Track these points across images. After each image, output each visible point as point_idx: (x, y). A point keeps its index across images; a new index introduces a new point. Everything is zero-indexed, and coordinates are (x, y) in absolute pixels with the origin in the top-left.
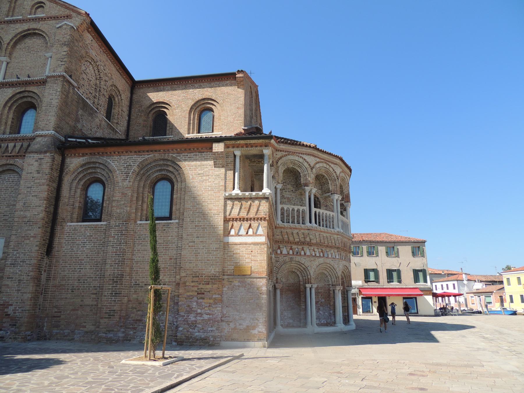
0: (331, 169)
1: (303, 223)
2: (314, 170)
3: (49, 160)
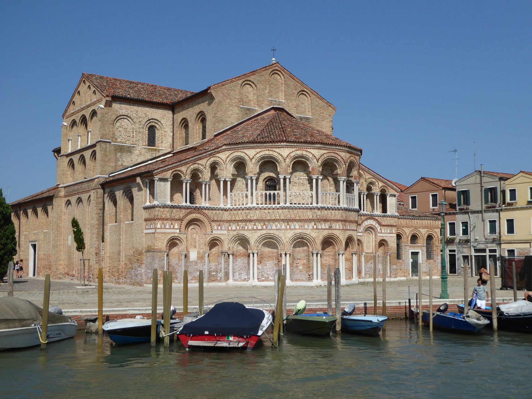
0: (275, 154)
2: (254, 160)
3: (95, 193)
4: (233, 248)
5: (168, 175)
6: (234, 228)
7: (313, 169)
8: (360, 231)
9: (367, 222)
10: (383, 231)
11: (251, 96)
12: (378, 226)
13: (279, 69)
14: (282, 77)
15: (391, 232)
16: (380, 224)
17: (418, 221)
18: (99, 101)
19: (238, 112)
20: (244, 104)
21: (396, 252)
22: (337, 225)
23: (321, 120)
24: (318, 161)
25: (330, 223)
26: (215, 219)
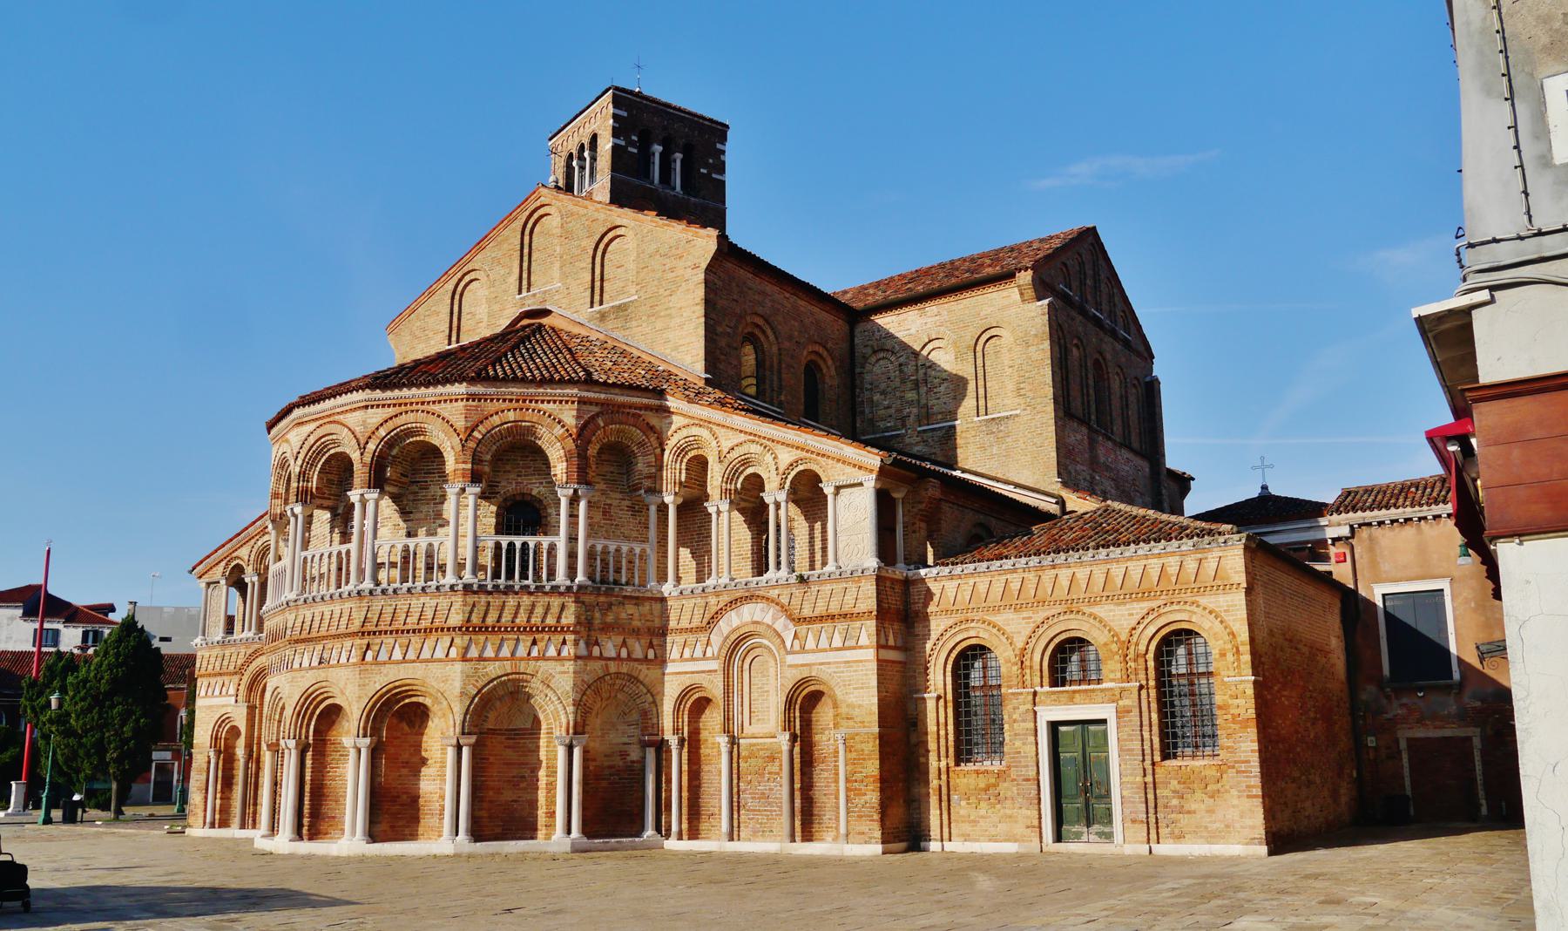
8: (709, 654)
10: (810, 644)
12: (786, 627)
15: (853, 643)
21: (876, 730)
23: (668, 292)
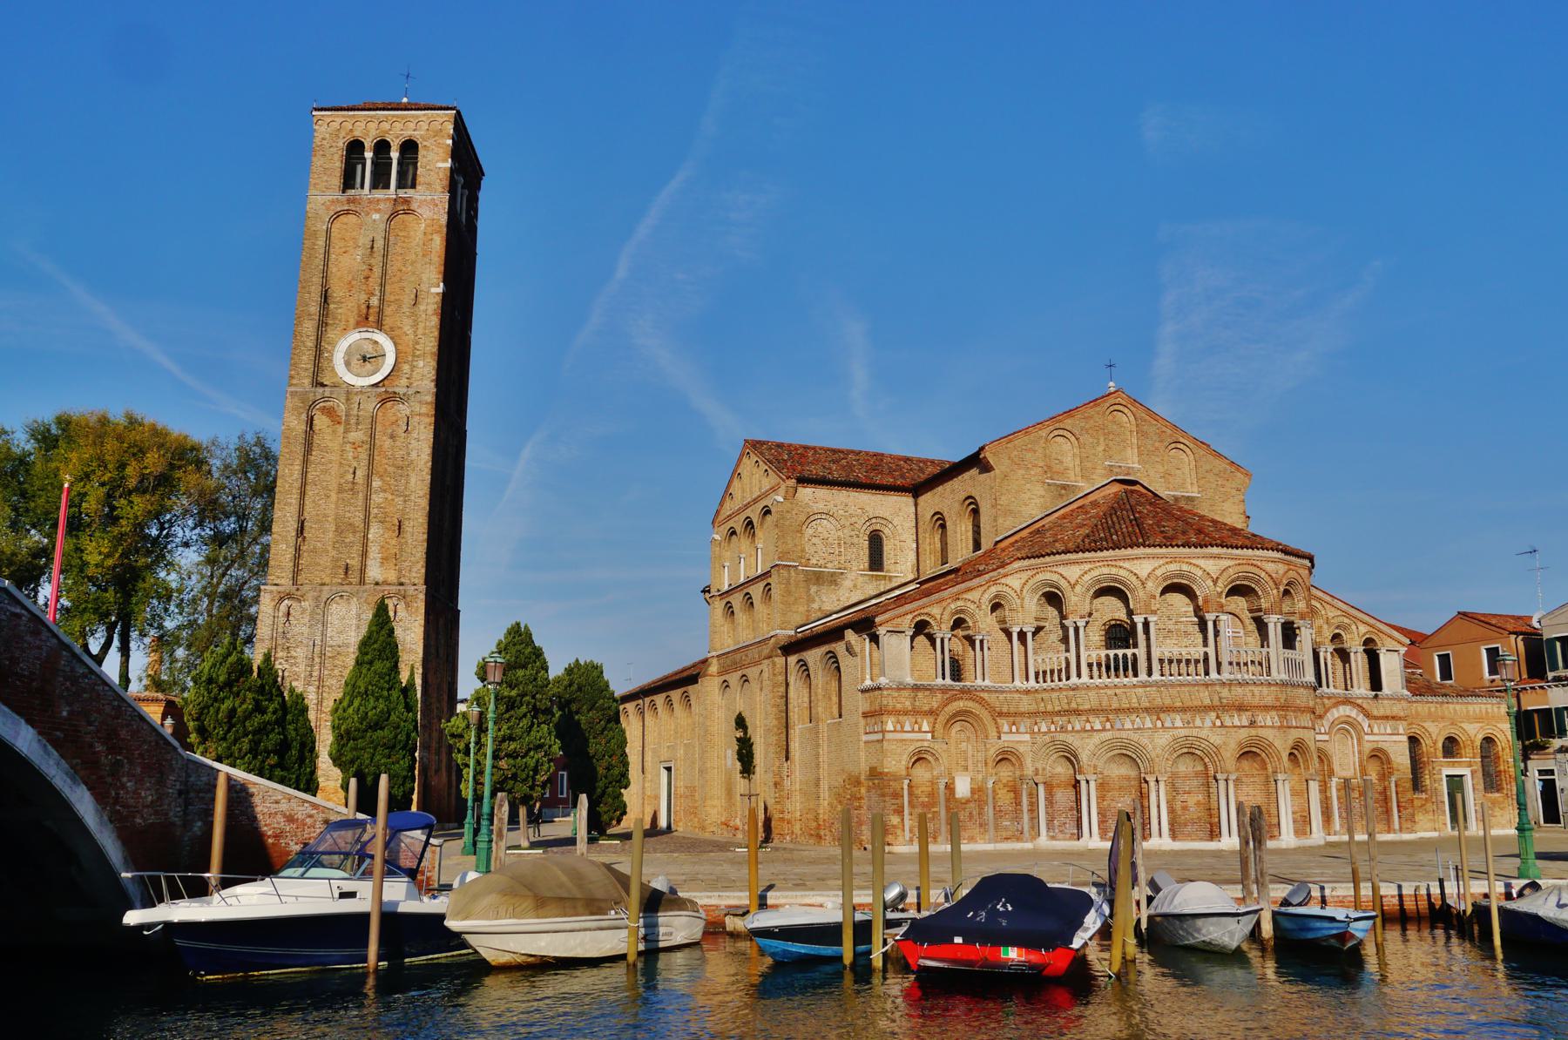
0: (1122, 573)
1: (1068, 678)
2: (1078, 589)
4: (1044, 769)
5: (907, 624)
6: (1044, 729)
7: (1206, 601)
8: (1323, 731)
9: (1338, 711)
10: (1376, 730)
11: (1068, 461)
13: (1124, 403)
14: (1132, 418)
16: (1368, 715)
17: (1458, 707)
18: (774, 489)
19: (1043, 493)
20: (1055, 477)
22: (1270, 719)
24: (1215, 582)
25: (1250, 713)
26: (1005, 710)
